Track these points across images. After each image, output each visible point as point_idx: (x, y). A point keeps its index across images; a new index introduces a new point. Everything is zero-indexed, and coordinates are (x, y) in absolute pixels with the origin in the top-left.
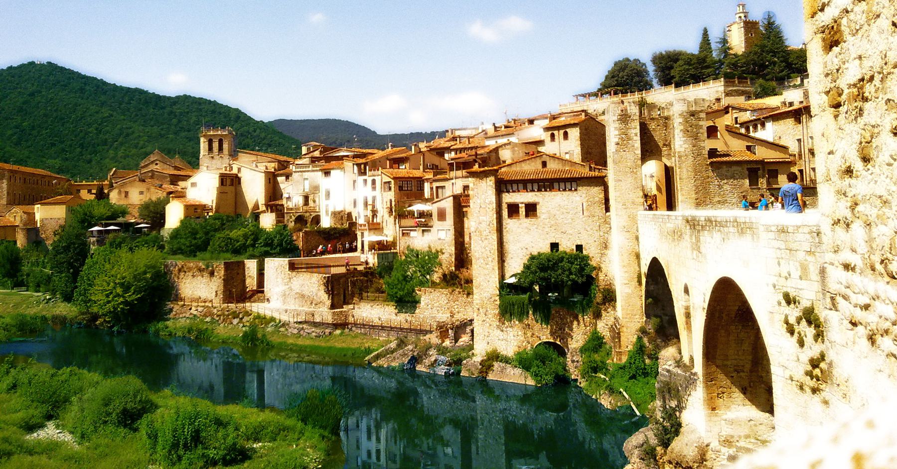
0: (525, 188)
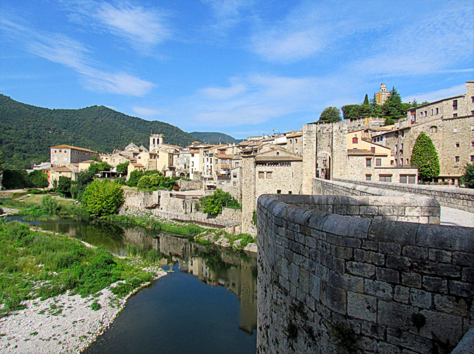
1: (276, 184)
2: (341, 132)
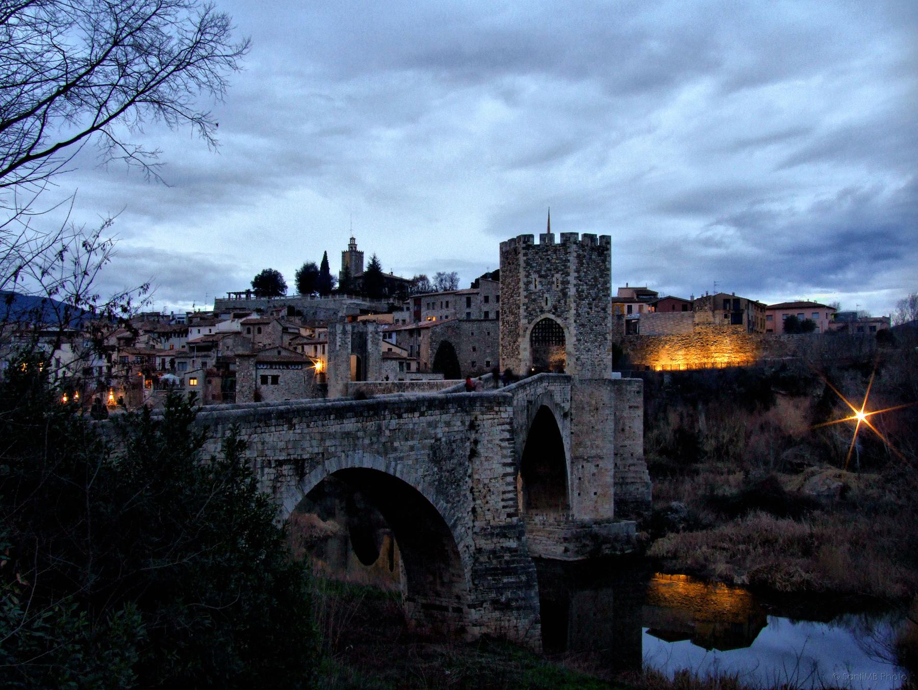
0: (271, 368)
1: (283, 391)
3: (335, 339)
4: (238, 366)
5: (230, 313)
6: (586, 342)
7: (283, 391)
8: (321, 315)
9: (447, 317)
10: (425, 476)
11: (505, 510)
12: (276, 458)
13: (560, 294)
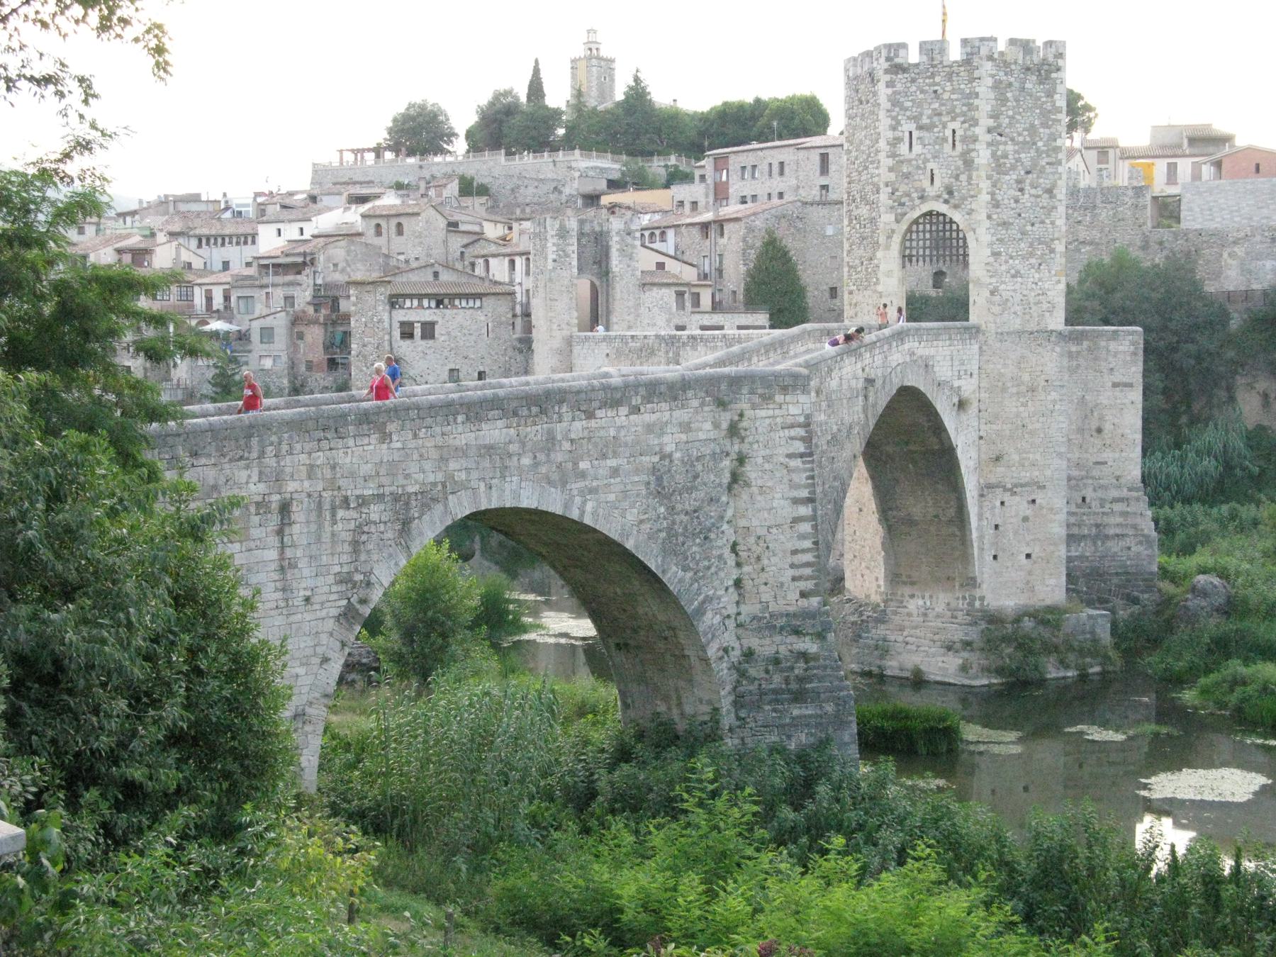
0: (421, 306)
1: (446, 353)
2: (629, 234)
3: (544, 247)
4: (354, 305)
5: (339, 194)
6: (1011, 258)
7: (446, 353)
8: (528, 193)
9: (781, 195)
10: (641, 522)
11: (797, 584)
12: (358, 492)
13: (960, 163)
